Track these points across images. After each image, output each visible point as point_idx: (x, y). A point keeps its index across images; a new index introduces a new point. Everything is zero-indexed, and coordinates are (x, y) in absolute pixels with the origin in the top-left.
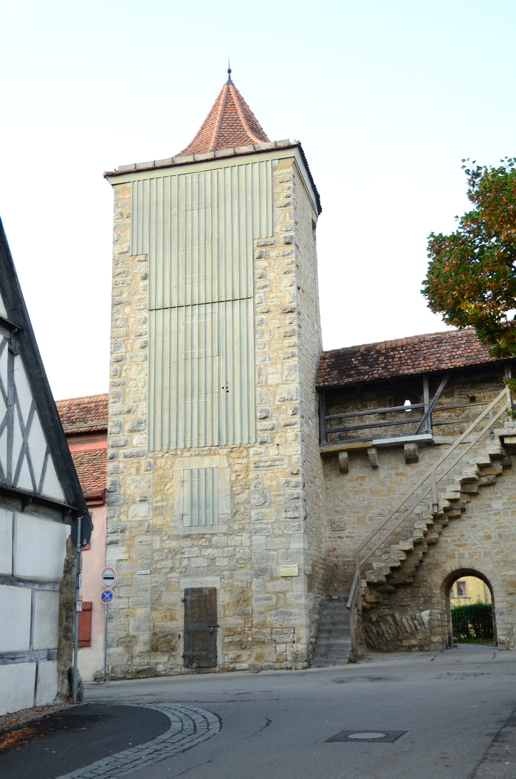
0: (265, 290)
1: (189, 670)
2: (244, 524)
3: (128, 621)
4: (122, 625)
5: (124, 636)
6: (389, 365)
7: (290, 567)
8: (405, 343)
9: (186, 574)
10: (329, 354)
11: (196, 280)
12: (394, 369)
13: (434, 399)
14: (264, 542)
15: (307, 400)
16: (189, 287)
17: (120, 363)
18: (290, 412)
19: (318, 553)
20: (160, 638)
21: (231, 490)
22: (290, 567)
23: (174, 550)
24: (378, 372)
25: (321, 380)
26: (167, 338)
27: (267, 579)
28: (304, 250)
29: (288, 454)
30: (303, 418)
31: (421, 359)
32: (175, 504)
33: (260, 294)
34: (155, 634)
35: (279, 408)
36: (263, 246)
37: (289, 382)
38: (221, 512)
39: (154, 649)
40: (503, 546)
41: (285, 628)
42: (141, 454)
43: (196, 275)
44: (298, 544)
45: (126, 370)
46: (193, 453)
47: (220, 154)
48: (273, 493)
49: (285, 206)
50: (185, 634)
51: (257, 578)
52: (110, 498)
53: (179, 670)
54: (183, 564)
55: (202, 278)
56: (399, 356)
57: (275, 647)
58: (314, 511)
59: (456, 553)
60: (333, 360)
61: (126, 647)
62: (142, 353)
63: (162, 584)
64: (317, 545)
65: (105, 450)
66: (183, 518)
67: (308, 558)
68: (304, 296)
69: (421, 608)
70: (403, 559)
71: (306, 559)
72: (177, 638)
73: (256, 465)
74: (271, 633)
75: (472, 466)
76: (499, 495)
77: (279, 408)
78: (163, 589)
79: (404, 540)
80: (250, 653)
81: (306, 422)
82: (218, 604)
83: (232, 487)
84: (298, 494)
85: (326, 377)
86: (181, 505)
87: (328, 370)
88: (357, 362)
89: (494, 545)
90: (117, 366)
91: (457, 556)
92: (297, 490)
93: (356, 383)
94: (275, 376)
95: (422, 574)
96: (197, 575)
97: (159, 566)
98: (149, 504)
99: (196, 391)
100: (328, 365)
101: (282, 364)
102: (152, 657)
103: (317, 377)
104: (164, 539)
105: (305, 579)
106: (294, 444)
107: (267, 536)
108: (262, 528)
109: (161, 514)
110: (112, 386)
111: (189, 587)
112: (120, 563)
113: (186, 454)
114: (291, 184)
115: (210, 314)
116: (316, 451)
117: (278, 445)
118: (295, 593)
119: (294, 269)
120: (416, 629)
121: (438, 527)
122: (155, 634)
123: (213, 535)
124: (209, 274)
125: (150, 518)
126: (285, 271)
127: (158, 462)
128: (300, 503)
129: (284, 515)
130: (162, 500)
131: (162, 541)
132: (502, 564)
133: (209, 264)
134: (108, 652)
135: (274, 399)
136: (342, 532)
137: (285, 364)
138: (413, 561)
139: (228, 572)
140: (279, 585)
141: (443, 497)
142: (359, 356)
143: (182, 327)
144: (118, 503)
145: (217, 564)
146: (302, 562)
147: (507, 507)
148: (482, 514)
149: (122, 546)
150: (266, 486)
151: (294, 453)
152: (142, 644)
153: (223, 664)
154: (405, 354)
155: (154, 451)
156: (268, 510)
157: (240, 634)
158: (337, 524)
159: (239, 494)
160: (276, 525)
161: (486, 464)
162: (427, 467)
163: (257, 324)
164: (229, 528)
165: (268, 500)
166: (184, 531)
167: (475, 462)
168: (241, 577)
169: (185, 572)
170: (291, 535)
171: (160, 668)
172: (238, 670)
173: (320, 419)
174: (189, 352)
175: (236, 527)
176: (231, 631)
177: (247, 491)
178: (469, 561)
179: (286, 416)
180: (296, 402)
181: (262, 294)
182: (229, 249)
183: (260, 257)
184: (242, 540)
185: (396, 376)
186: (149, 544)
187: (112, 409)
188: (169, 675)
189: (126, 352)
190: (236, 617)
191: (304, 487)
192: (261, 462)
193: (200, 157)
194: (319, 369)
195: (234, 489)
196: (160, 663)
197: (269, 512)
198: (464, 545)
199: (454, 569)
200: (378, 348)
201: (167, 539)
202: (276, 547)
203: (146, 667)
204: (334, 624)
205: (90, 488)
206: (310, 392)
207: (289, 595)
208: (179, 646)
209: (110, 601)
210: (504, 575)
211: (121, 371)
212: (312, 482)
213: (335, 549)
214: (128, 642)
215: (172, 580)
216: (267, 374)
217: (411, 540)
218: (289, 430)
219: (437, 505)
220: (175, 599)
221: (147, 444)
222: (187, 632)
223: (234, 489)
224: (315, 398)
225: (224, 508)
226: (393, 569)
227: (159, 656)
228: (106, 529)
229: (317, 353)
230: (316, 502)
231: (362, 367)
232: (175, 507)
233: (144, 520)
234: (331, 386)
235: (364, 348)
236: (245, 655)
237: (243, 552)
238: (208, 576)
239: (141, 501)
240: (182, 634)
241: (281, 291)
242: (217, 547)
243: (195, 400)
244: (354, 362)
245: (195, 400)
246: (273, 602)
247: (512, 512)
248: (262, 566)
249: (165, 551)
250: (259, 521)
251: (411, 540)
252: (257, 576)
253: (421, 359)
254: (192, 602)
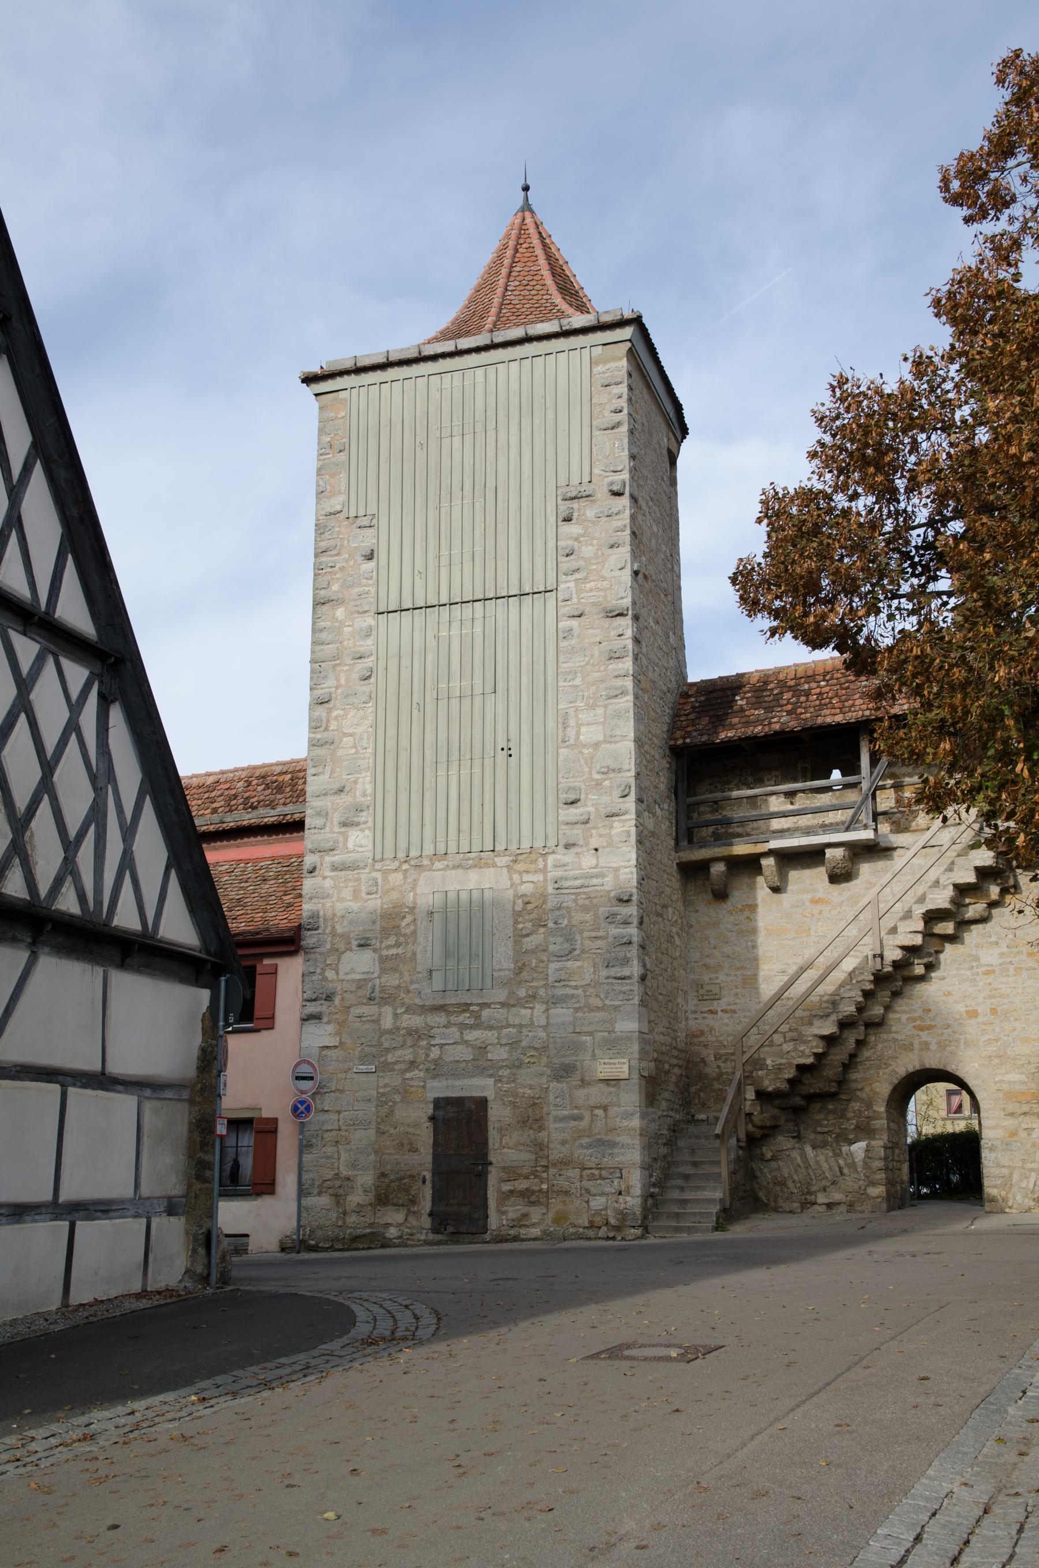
0: (577, 576)
1: (440, 1237)
2: (537, 987)
3: (338, 1152)
4: (328, 1157)
5: (330, 1177)
6: (800, 707)
7: (614, 1064)
8: (829, 668)
9: (435, 1072)
10: (695, 689)
11: (456, 559)
12: (808, 715)
13: (878, 768)
14: (571, 1018)
15: (651, 771)
16: (444, 572)
17: (326, 705)
18: (617, 793)
19: (670, 1040)
20: (392, 1181)
21: (515, 929)
22: (614, 1064)
23: (417, 1031)
24: (781, 721)
25: (679, 734)
26: (406, 662)
27: (575, 1083)
28: (651, 503)
29: (614, 865)
30: (642, 802)
31: (857, 696)
32: (418, 952)
33: (568, 584)
34: (383, 1175)
35: (599, 784)
36: (575, 498)
37: (617, 739)
38: (497, 967)
39: (382, 1199)
40: (998, 1030)
41: (604, 1169)
42: (362, 865)
43: (456, 551)
44: (629, 1025)
45: (336, 718)
46: (450, 864)
47: (500, 337)
48: (586, 934)
49: (613, 428)
50: (433, 1176)
51: (558, 1081)
52: (309, 939)
53: (423, 1237)
54: (432, 1056)
55: (467, 557)
56: (818, 690)
57: (588, 1202)
58: (663, 966)
59: (916, 1042)
60: (702, 698)
61: (336, 1196)
62: (364, 688)
63: (395, 1090)
64: (667, 1025)
65: (301, 856)
66: (431, 975)
67: (648, 1048)
68: (648, 586)
69: (851, 1137)
70: (820, 1050)
71: (643, 1051)
72: (421, 1183)
73: (556, 886)
74: (581, 1177)
75: (945, 887)
76: (993, 939)
77: (599, 784)
78: (398, 1098)
79: (822, 1017)
80: (544, 1211)
81: (649, 809)
82: (491, 1125)
83: (516, 922)
84: (631, 936)
85: (689, 729)
86: (429, 953)
87: (692, 716)
88: (744, 702)
89: (984, 1027)
90: (321, 711)
91: (916, 1046)
92: (628, 930)
93: (740, 739)
94: (593, 728)
95: (854, 1077)
96: (455, 1075)
97: (390, 1058)
98: (375, 951)
99: (455, 756)
100: (693, 707)
101: (606, 706)
102: (379, 1214)
103: (671, 731)
104: (399, 1011)
105: (640, 1085)
106: (625, 849)
107: (577, 1010)
108: (567, 995)
109: (394, 969)
110: (314, 745)
111: (441, 1096)
112: (324, 1053)
113: (438, 865)
114: (623, 389)
115: (482, 620)
116: (668, 859)
117: (596, 850)
118: (622, 1109)
119: (628, 539)
120: (842, 1173)
121: (884, 996)
122: (383, 1175)
123: (484, 1005)
124: (479, 548)
125: (376, 975)
126: (612, 542)
127: (390, 878)
128: (634, 952)
129: (604, 973)
130: (397, 945)
131: (396, 1015)
132: (996, 1061)
133: (478, 532)
134: (303, 1202)
135: (591, 768)
136: (715, 1002)
137: (610, 707)
138: (839, 1056)
139: (509, 1071)
140: (596, 1094)
141: (891, 943)
142: (749, 692)
143: (431, 642)
144: (322, 950)
145: (490, 1056)
146: (637, 1056)
147: (1008, 960)
148: (963, 972)
149: (329, 1023)
150: (574, 923)
151: (624, 864)
152: (360, 1191)
153: (499, 1229)
154: (828, 688)
155: (382, 860)
156: (579, 964)
157: (527, 1177)
158: (707, 987)
159: (528, 935)
160: (591, 990)
161: (969, 884)
162: (866, 888)
163: (561, 636)
164: (512, 994)
165: (578, 947)
166: (434, 999)
167: (950, 881)
168: (531, 1080)
169: (436, 1069)
170: (616, 1008)
171: (392, 1232)
172: (523, 1240)
173: (677, 803)
174: (443, 685)
175: (522, 993)
176: (512, 1172)
177: (542, 930)
178: (938, 1055)
179: (610, 800)
180: (629, 774)
181: (572, 585)
182: (513, 506)
183: (568, 519)
184: (532, 1015)
185: (811, 728)
186: (373, 1021)
187: (313, 785)
188: (407, 1246)
189: (337, 687)
190: (521, 1148)
191: (641, 923)
192: (566, 879)
193: (465, 343)
194: (676, 716)
195: (520, 926)
196: (390, 1225)
197: (579, 967)
198: (930, 1027)
199: (911, 1069)
200: (781, 677)
201: (404, 1013)
202: (590, 1029)
203: (368, 1231)
204: (695, 1164)
205: (277, 922)
206: (657, 756)
207: (613, 1111)
208: (424, 1197)
209: (306, 1117)
210: (1000, 1081)
211: (328, 720)
212: (659, 915)
213: (702, 1033)
214: (338, 1189)
215: (411, 1083)
216: (579, 725)
217: (834, 1017)
218: (616, 824)
219: (881, 956)
220: (416, 1117)
221: (370, 847)
222: (436, 1172)
223: (520, 926)
224: (668, 766)
225: (503, 958)
226: (801, 1068)
227: (389, 1213)
228: (300, 993)
229: (673, 685)
230: (667, 949)
231: (752, 711)
232: (419, 956)
233: (364, 980)
234: (696, 745)
235: (757, 678)
236: (536, 1214)
237: (534, 1036)
238: (473, 1076)
239: (360, 946)
240: (428, 1176)
241: (604, 579)
242: (490, 1028)
243: (454, 772)
244: (739, 703)
245: (454, 772)
246: (584, 1124)
247: (1015, 969)
248: (567, 1060)
249: (402, 1032)
250: (562, 983)
251: (834, 1017)
252: (558, 1078)
253: (857, 696)
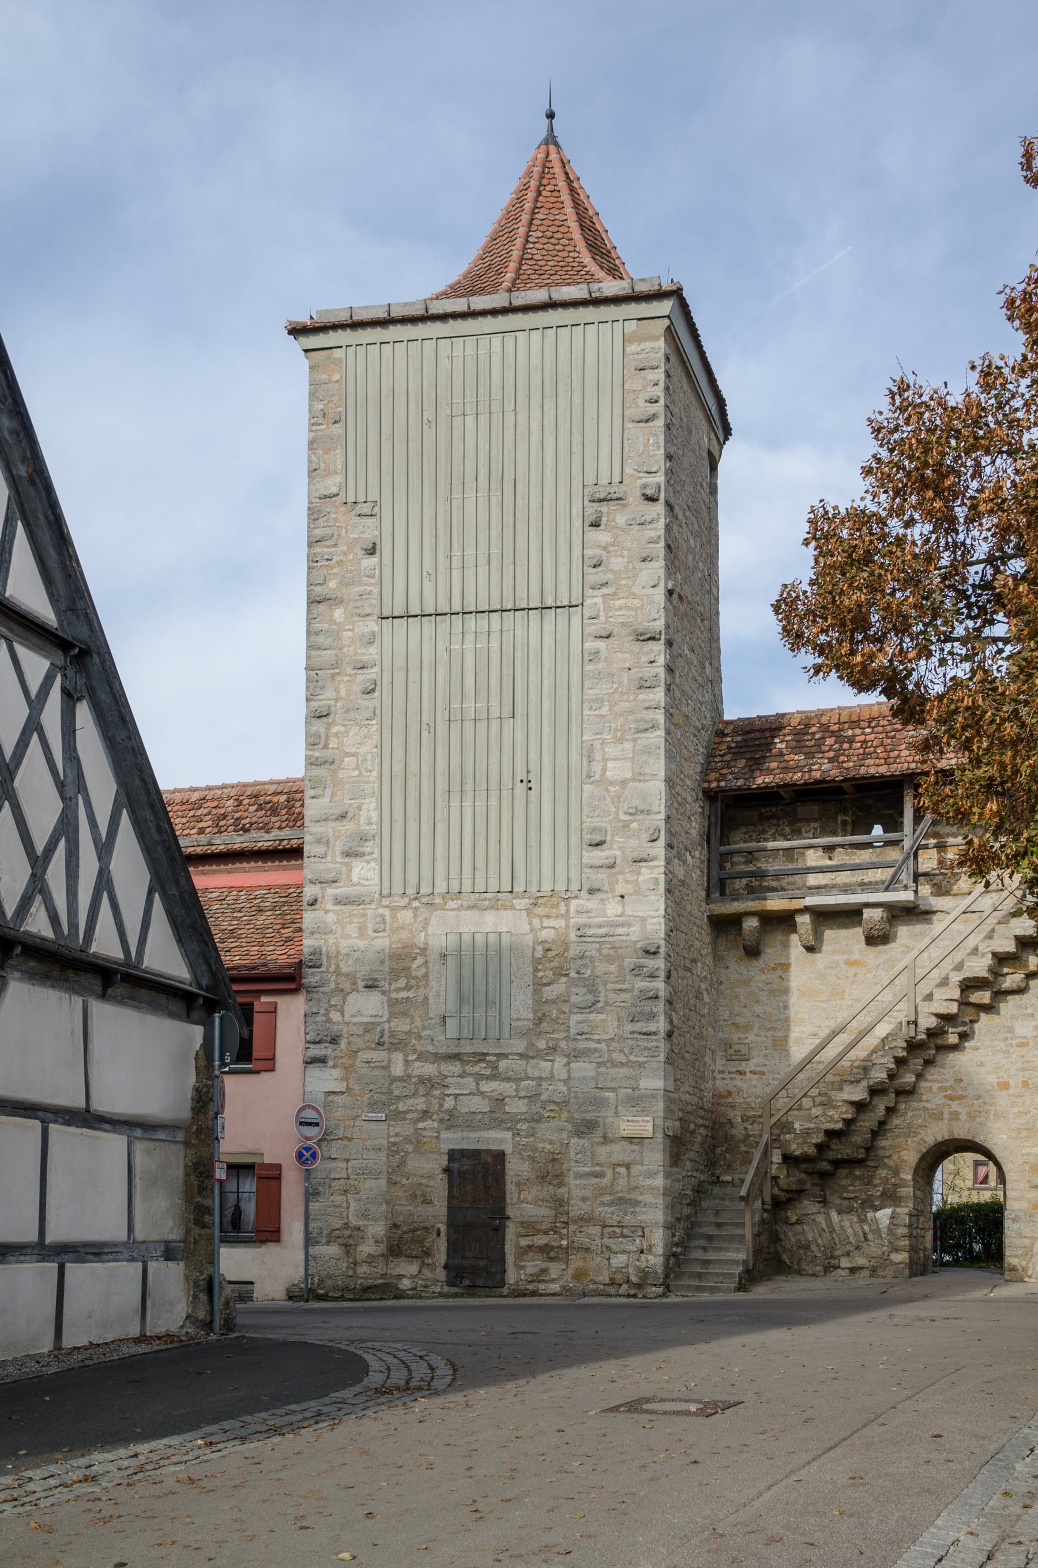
63: (407, 1140)
222: (451, 1224)
240: (443, 1228)
254: (462, 1174)
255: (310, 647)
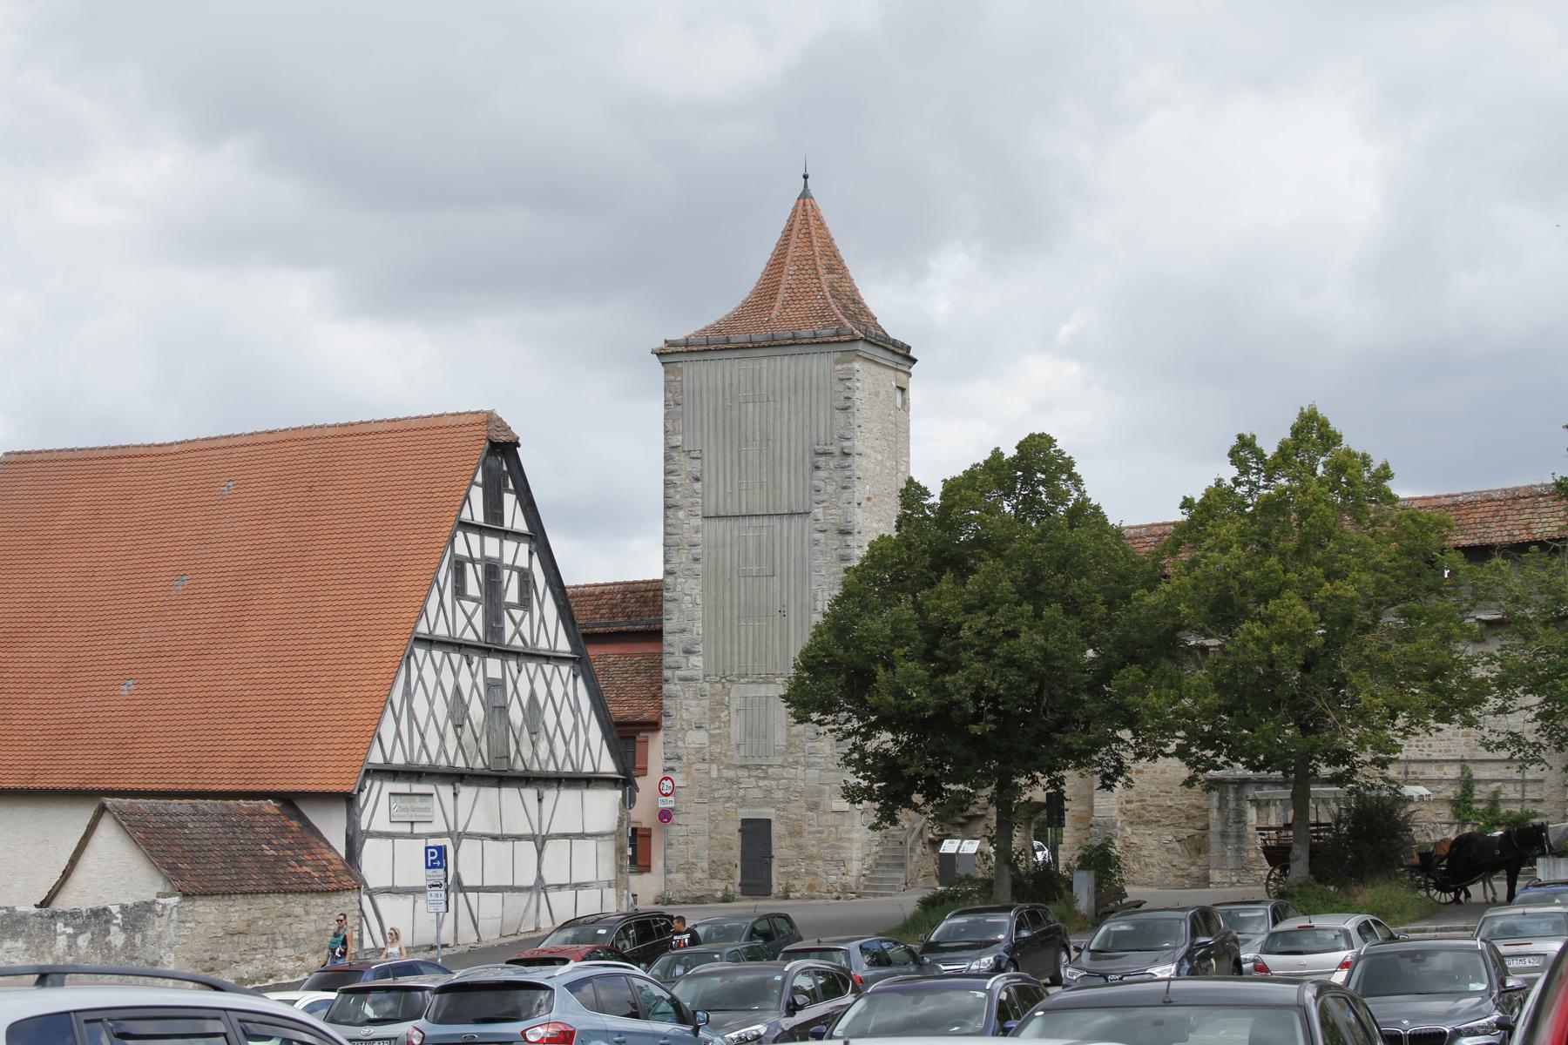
169: (743, 802)
255: (666, 534)
